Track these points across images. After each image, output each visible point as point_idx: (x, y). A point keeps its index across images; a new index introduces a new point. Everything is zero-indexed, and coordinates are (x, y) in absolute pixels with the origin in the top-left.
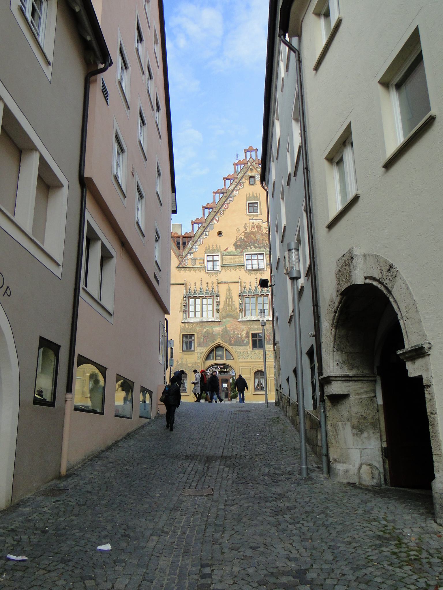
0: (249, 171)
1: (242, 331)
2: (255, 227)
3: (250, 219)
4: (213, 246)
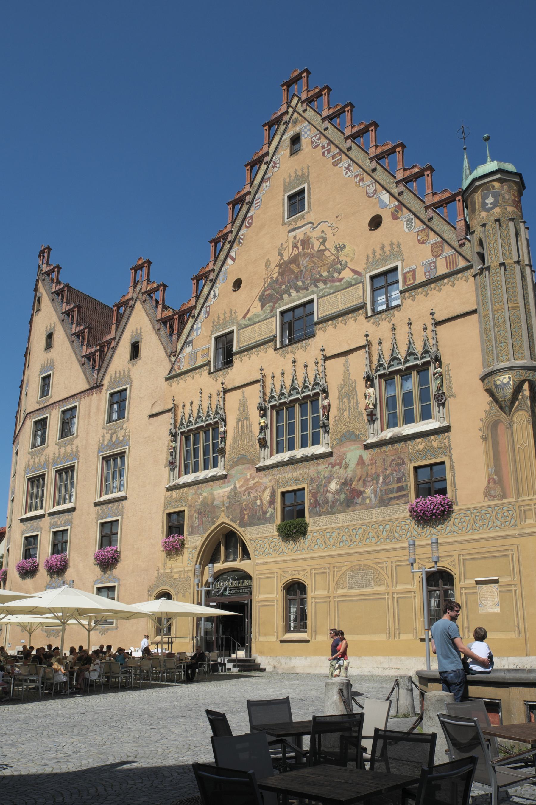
0: (290, 125)
1: (264, 490)
2: (299, 245)
3: (290, 231)
4: (225, 314)
